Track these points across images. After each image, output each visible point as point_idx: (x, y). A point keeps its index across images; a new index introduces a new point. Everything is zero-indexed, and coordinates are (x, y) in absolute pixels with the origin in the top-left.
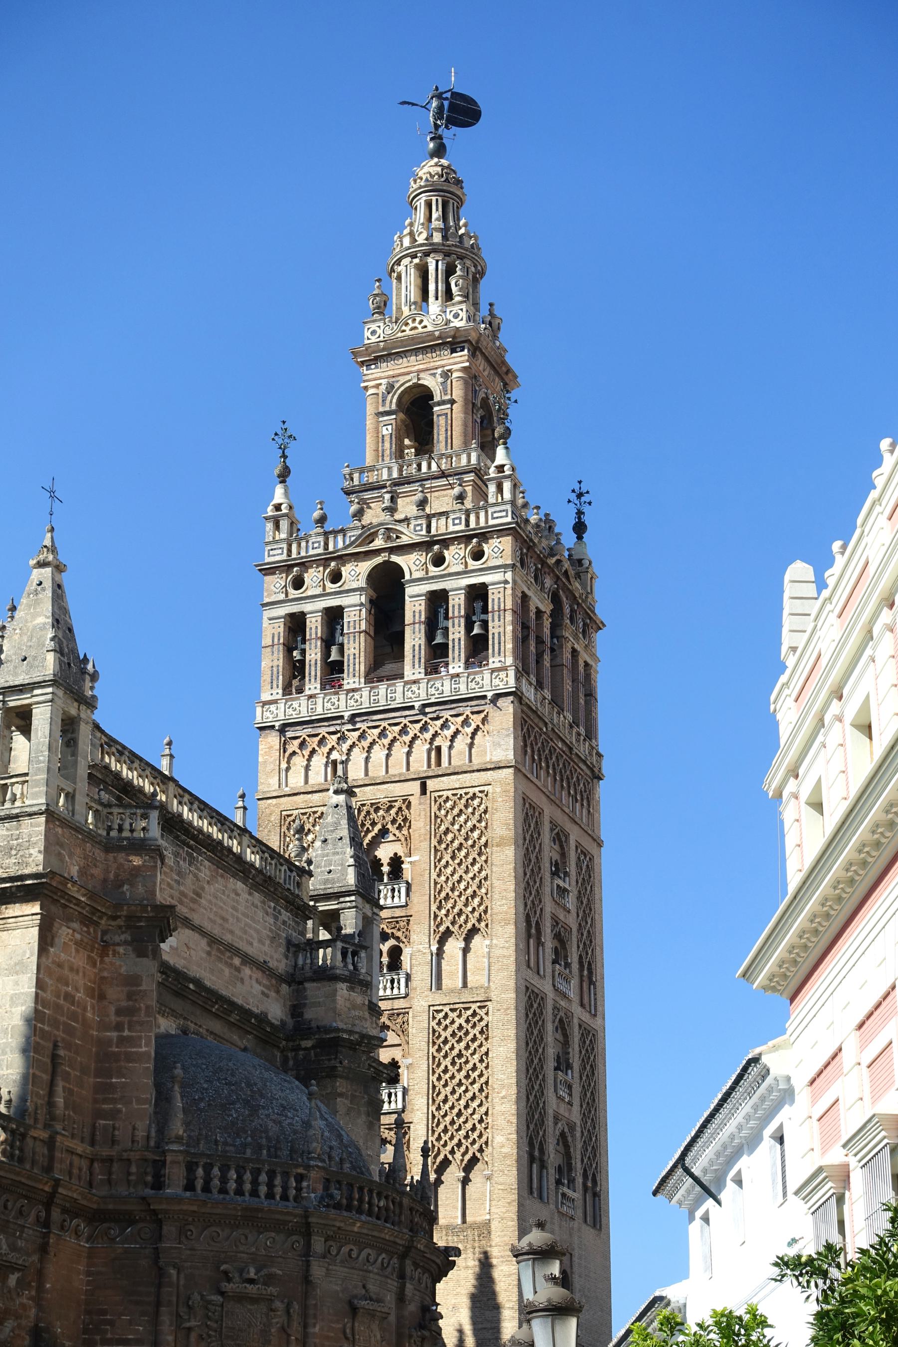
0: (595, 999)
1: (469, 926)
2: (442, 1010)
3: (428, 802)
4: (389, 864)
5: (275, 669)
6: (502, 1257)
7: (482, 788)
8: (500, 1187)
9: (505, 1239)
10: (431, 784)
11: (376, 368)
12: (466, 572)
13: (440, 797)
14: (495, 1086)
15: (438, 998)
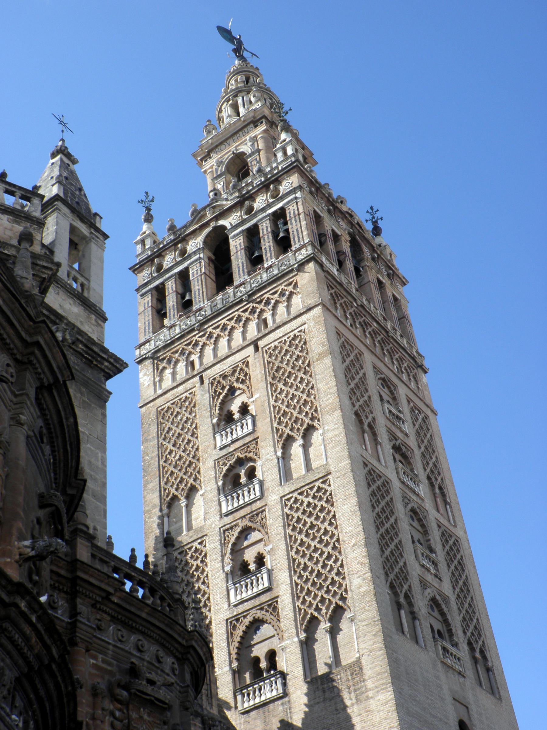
0: (453, 516)
1: (305, 426)
2: (291, 497)
3: (261, 355)
4: (239, 412)
5: (147, 323)
6: (376, 687)
7: (300, 329)
8: (364, 623)
9: (377, 669)
10: (261, 343)
11: (210, 158)
12: (269, 206)
13: (269, 349)
14: (346, 539)
15: (287, 488)
